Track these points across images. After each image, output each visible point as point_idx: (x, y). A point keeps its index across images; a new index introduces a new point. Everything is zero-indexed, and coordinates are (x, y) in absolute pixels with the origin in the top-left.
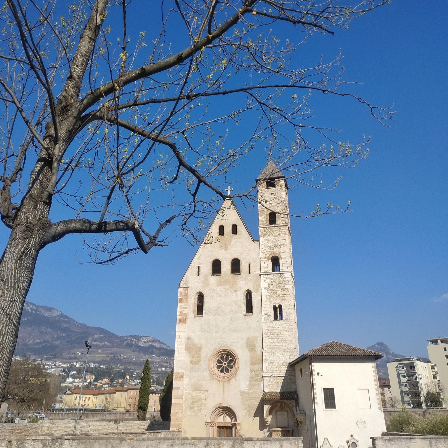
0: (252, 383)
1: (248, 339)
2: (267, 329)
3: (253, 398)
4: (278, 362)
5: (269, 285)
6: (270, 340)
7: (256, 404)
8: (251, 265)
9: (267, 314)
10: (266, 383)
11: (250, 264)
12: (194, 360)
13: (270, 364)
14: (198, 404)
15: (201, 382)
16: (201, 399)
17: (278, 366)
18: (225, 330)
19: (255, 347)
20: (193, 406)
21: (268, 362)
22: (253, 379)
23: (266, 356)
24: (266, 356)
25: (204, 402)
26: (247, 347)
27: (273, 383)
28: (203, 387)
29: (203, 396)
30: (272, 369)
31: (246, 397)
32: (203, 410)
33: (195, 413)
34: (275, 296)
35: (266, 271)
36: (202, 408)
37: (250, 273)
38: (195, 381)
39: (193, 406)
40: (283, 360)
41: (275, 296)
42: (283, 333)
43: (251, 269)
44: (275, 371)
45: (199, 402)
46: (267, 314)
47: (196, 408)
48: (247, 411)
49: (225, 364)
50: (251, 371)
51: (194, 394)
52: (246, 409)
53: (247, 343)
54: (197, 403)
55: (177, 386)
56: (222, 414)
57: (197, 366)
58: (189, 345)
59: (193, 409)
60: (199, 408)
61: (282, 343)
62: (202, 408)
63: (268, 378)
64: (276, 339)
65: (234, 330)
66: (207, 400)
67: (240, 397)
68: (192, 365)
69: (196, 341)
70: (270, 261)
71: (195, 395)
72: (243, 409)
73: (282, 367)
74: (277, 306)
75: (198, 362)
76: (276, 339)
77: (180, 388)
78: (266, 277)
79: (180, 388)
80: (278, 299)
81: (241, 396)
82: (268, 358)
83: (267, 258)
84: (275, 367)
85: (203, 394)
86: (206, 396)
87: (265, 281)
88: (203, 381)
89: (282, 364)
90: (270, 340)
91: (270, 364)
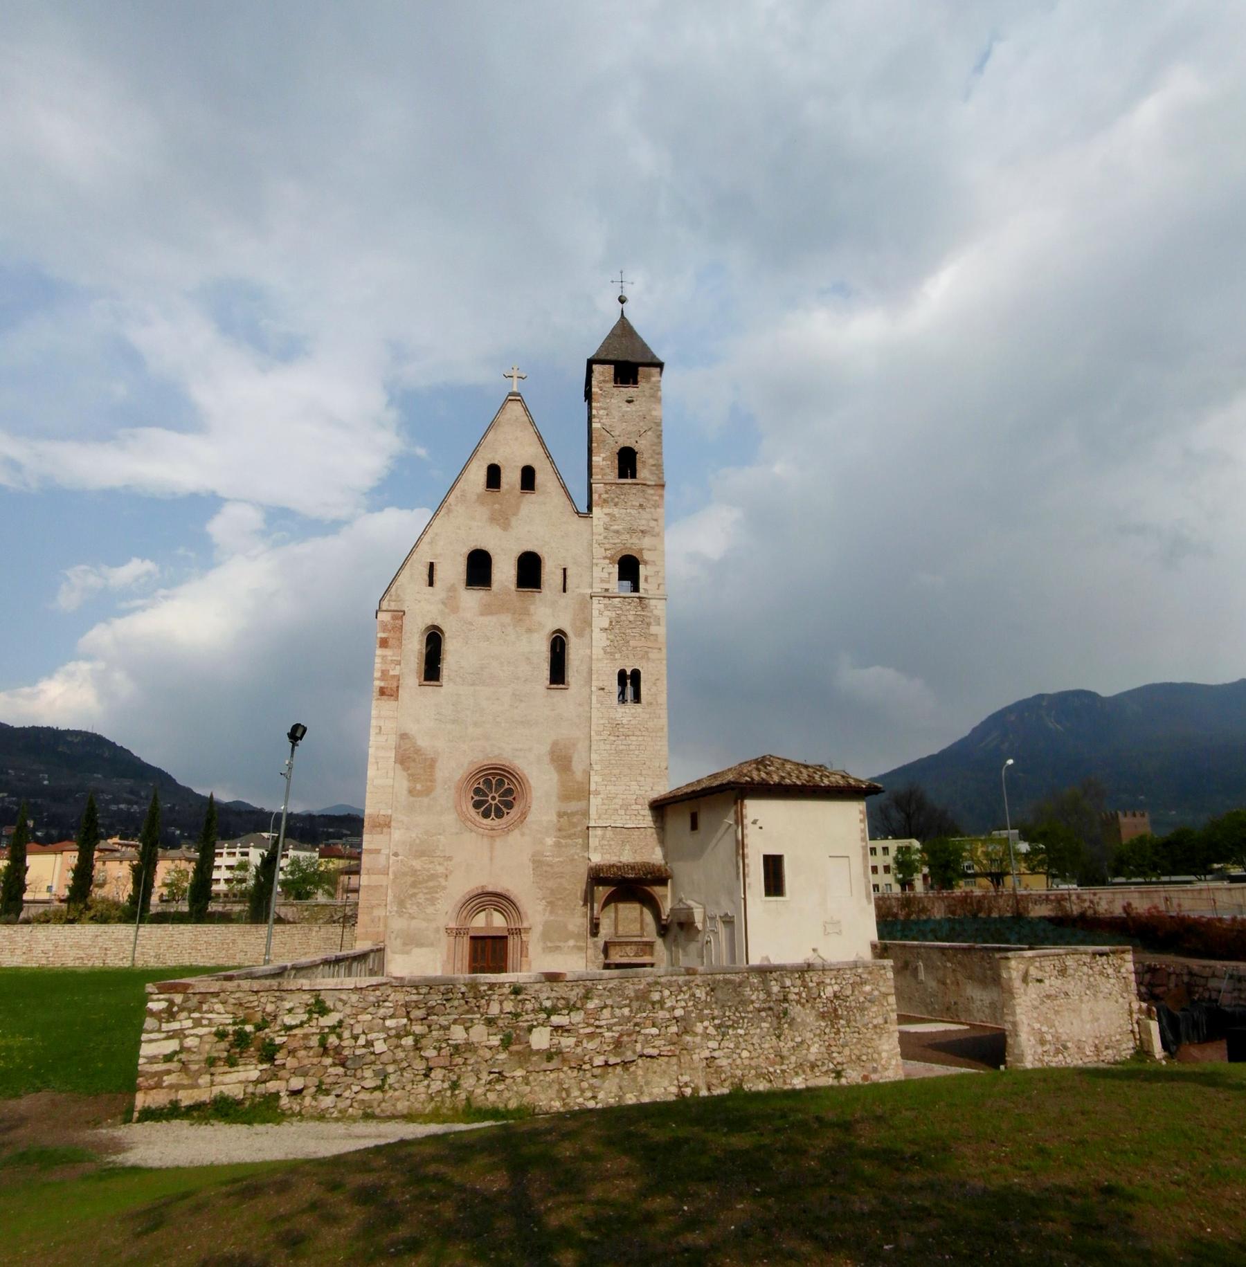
0: (562, 841)
2: (602, 722)
3: (562, 873)
4: (625, 797)
5: (611, 622)
7: (568, 887)
8: (568, 573)
9: (603, 689)
10: (593, 842)
11: (565, 570)
12: (419, 787)
13: (605, 801)
14: (427, 888)
15: (434, 838)
16: (433, 877)
17: (626, 807)
18: (498, 719)
19: (571, 762)
20: (416, 891)
21: (602, 796)
22: (564, 833)
23: (596, 783)
24: (596, 783)
26: (553, 760)
27: (612, 843)
28: (441, 848)
29: (440, 869)
31: (546, 872)
32: (439, 901)
33: (418, 907)
34: (624, 648)
35: (607, 590)
36: (437, 896)
37: (565, 591)
38: (420, 836)
39: (416, 891)
40: (638, 792)
41: (624, 648)
42: (638, 733)
43: (567, 580)
44: (617, 816)
45: (431, 884)
46: (603, 689)
47: (420, 895)
48: (547, 902)
49: (494, 798)
51: (417, 864)
52: (544, 898)
54: (424, 885)
55: (373, 847)
56: (484, 910)
57: (426, 800)
58: (405, 750)
59: (413, 899)
60: (428, 896)
61: (638, 756)
62: (437, 896)
63: (599, 832)
64: (623, 747)
65: (522, 722)
66: (450, 878)
67: (532, 872)
68: (412, 799)
69: (423, 742)
70: (617, 566)
71: (419, 868)
72: (538, 899)
73: (633, 807)
74: (629, 673)
75: (428, 791)
76: (623, 747)
77: (380, 850)
78: (605, 602)
79: (380, 850)
80: (631, 656)
81: (533, 869)
82: (601, 788)
83: (609, 559)
84: (618, 807)
85: (439, 864)
86: (447, 869)
87: (601, 613)
88: (440, 834)
89: (634, 801)
90: (608, 747)
91: (605, 801)
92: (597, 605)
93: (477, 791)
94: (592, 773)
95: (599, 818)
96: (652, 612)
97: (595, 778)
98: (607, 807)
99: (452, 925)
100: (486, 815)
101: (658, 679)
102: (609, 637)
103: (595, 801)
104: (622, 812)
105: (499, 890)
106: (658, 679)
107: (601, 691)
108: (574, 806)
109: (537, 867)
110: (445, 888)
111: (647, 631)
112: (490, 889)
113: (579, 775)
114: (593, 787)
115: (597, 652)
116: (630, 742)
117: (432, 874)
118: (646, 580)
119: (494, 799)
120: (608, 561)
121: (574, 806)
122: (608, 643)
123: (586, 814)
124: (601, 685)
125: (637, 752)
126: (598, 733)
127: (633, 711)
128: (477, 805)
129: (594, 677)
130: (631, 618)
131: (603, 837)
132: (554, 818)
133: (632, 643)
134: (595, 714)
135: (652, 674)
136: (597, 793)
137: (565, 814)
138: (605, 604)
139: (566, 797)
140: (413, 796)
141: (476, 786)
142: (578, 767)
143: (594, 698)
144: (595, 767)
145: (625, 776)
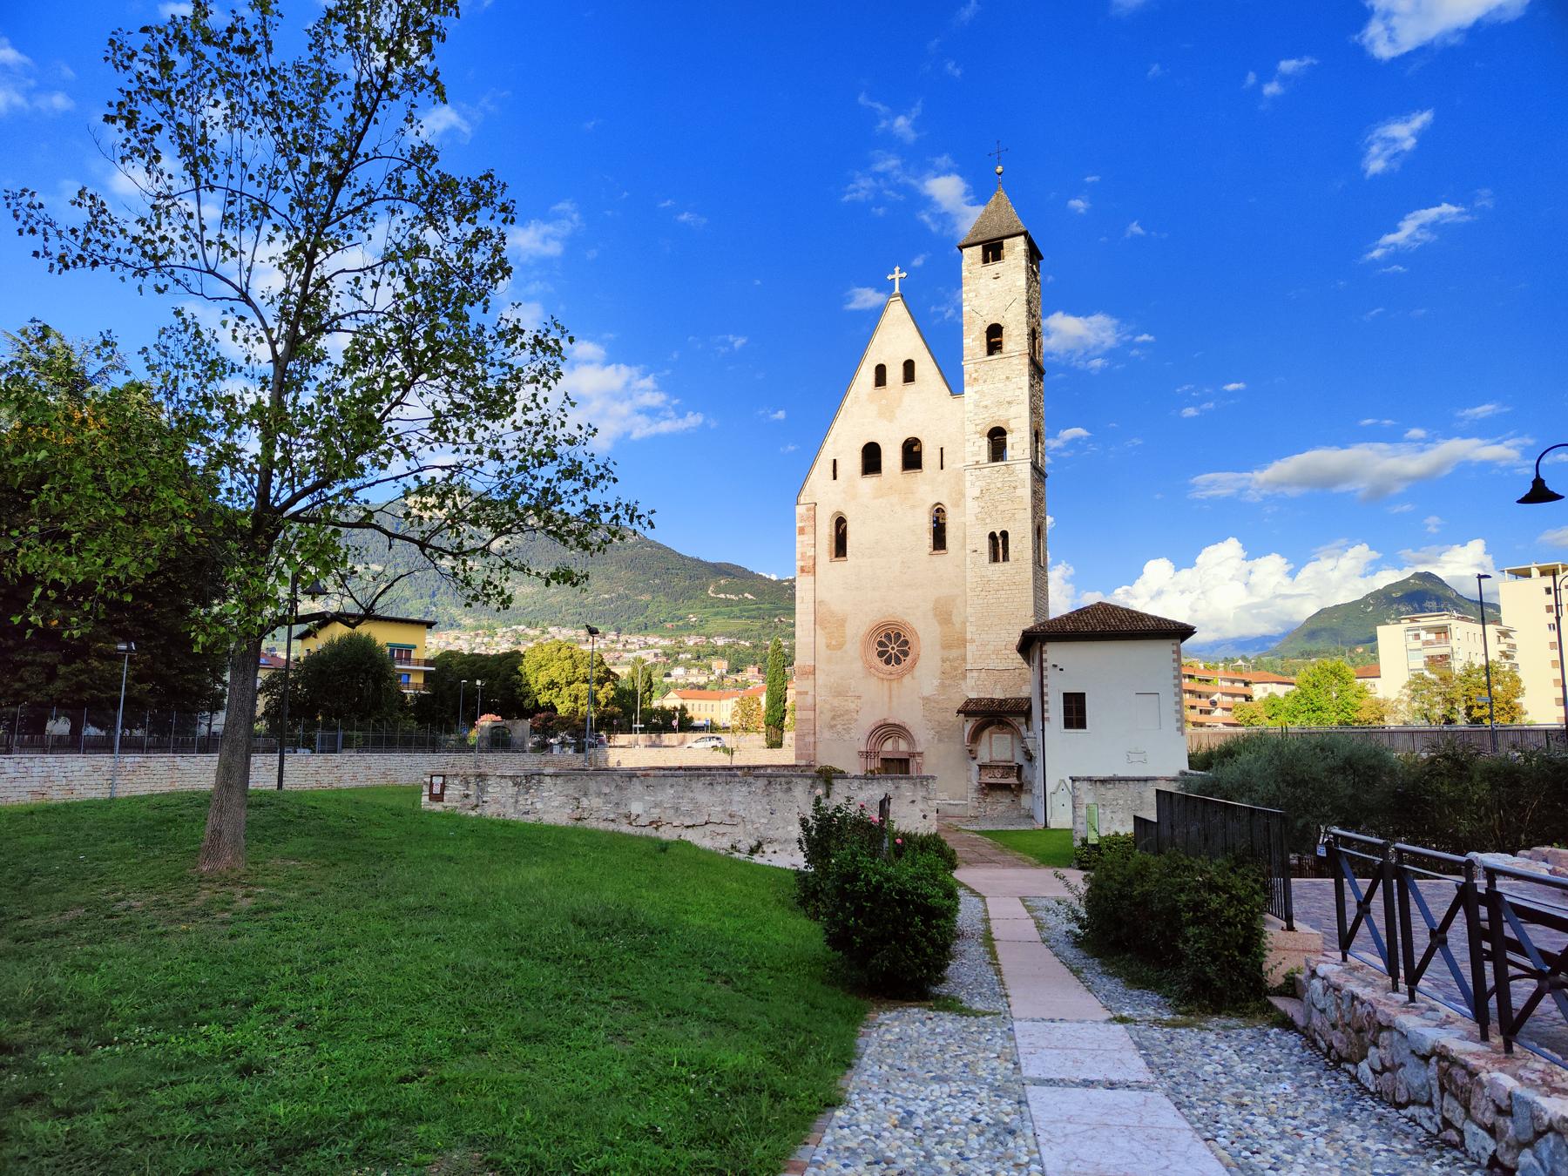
12: (834, 643)
17: (997, 652)
26: (935, 615)
51: (836, 702)
53: (935, 609)
57: (839, 653)
63: (975, 674)
87: (973, 484)
92: (968, 477)
93: (881, 644)
99: (863, 749)
108: (955, 653)
112: (890, 721)
113: (958, 626)
114: (969, 636)
115: (970, 518)
119: (893, 649)
121: (955, 653)
123: (964, 659)
124: (974, 548)
126: (973, 590)
130: (999, 485)
136: (973, 641)
137: (948, 659)
139: (946, 646)
142: (957, 619)
144: (971, 619)
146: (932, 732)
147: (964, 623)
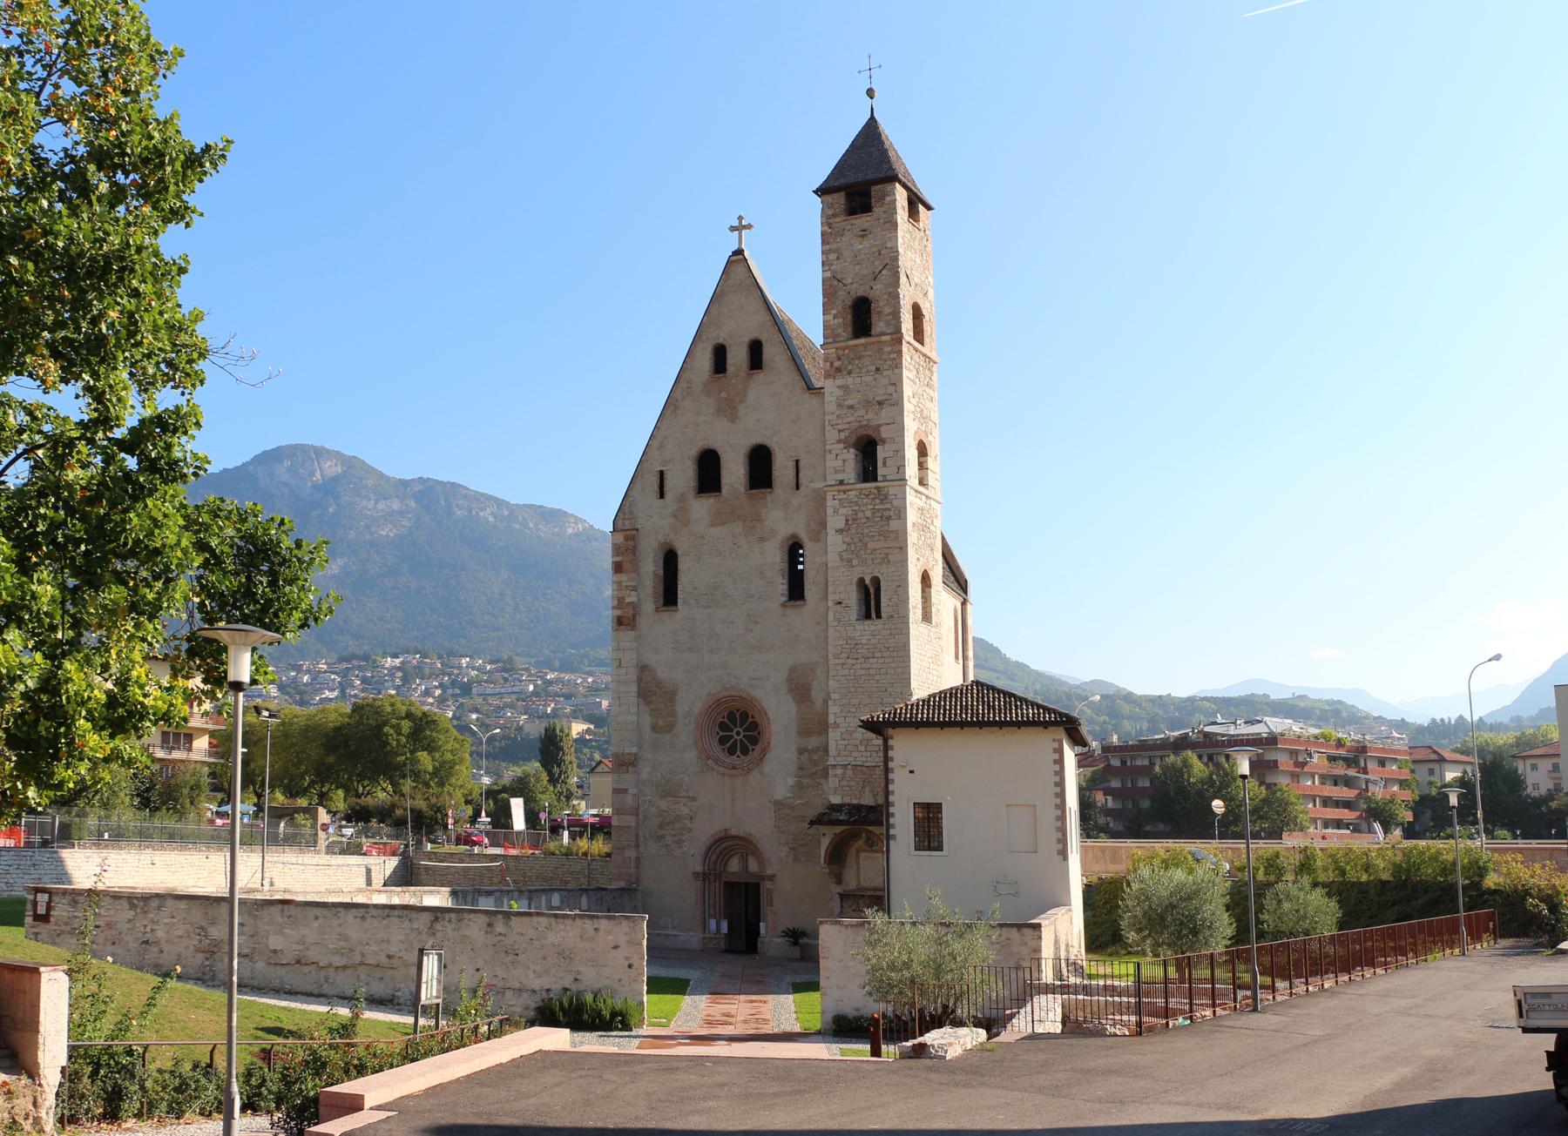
1: (792, 670)
2: (840, 642)
5: (847, 520)
6: (846, 672)
9: (840, 603)
11: (797, 462)
12: (661, 723)
16: (678, 818)
21: (841, 730)
25: (689, 825)
26: (790, 690)
29: (685, 811)
30: (849, 748)
31: (787, 815)
37: (798, 488)
42: (878, 655)
45: (677, 825)
46: (840, 603)
47: (668, 838)
50: (801, 751)
51: (663, 804)
52: (787, 844)
53: (790, 680)
57: (668, 737)
60: (676, 839)
61: (878, 681)
62: (684, 838)
68: (655, 736)
72: (780, 844)
75: (669, 728)
84: (858, 742)
87: (836, 512)
90: (846, 672)
94: (830, 703)
95: (839, 755)
96: (891, 503)
97: (833, 709)
98: (845, 742)
99: (699, 869)
100: (731, 751)
101: (899, 586)
102: (846, 539)
103: (833, 735)
104: (862, 748)
105: (741, 835)
106: (899, 586)
107: (838, 606)
108: (814, 742)
109: (779, 809)
110: (690, 830)
111: (886, 528)
113: (819, 705)
114: (831, 720)
115: (833, 558)
116: (869, 666)
117: (678, 816)
118: (884, 464)
119: (738, 734)
120: (841, 446)
121: (814, 742)
122: (844, 547)
125: (877, 677)
126: (837, 656)
127: (873, 628)
128: (722, 741)
129: (830, 589)
131: (843, 777)
132: (795, 755)
133: (871, 545)
134: (831, 633)
135: (893, 581)
136: (836, 725)
138: (840, 500)
139: (804, 732)
140: (656, 733)
141: (721, 720)
142: (817, 696)
143: (831, 614)
144: (834, 696)
145: (865, 706)
146: (786, 848)
147: (826, 702)
